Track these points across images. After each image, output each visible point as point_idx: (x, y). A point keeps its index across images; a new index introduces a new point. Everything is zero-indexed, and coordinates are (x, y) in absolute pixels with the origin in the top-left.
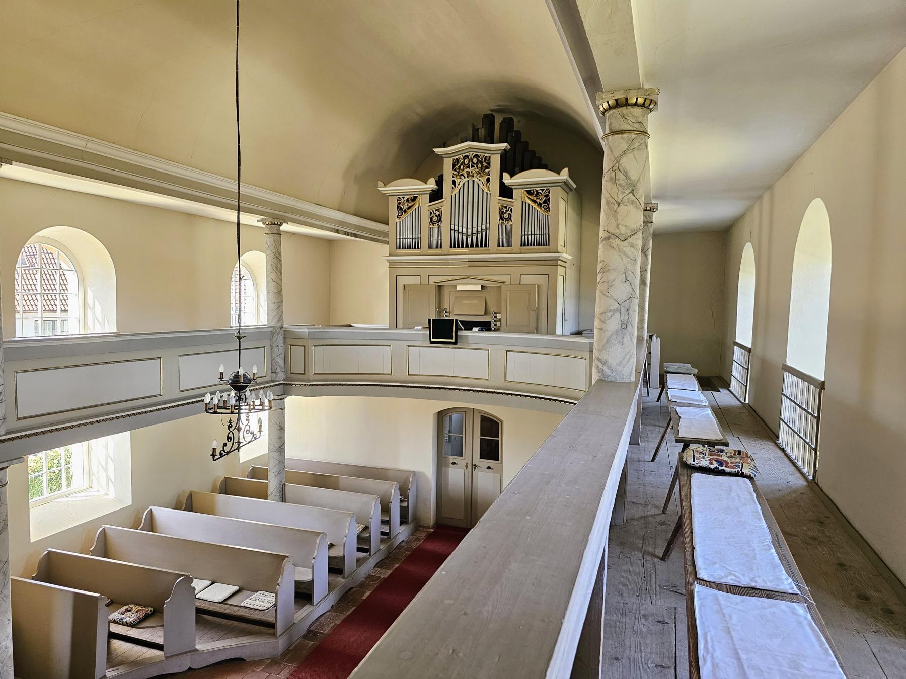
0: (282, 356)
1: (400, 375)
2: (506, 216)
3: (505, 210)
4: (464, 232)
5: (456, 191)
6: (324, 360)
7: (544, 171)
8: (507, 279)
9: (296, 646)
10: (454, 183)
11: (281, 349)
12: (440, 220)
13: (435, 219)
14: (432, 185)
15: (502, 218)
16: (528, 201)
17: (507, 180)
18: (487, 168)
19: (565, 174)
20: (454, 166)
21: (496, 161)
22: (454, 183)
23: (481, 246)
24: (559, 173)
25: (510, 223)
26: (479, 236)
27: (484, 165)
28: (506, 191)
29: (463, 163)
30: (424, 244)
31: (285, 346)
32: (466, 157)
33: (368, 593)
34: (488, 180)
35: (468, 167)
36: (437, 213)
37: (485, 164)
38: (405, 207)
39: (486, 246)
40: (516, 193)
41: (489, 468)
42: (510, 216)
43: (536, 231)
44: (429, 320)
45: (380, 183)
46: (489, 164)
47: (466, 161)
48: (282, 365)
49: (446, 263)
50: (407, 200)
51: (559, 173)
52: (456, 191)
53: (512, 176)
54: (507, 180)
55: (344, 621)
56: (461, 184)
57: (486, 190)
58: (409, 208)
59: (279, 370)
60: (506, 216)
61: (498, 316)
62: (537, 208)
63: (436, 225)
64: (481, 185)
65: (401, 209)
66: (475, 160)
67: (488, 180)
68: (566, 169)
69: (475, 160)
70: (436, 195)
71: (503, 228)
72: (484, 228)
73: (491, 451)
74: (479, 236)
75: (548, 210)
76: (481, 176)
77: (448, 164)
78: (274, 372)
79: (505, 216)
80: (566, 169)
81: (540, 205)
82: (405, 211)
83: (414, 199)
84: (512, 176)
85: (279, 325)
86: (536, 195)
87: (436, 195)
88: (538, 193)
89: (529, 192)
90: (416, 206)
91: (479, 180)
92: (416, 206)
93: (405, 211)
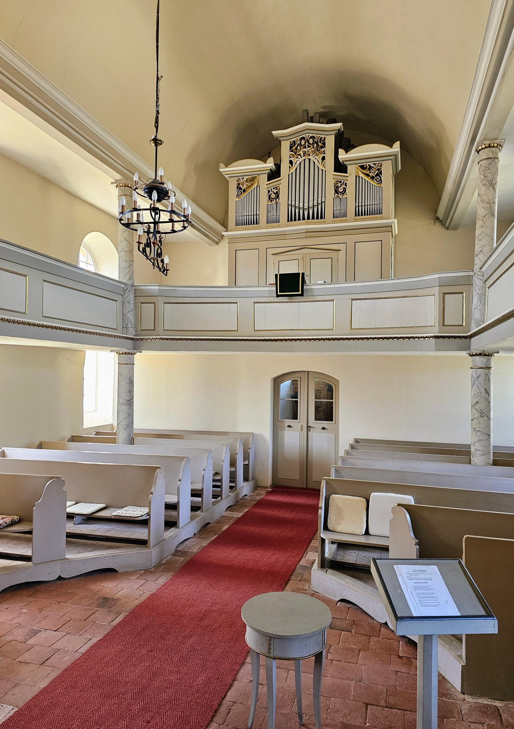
0: (133, 313)
1: (246, 332)
2: (341, 190)
3: (339, 184)
6: (174, 317)
7: (378, 145)
8: (342, 247)
9: (168, 561)
10: (291, 162)
11: (132, 306)
13: (273, 196)
14: (270, 164)
15: (336, 192)
16: (361, 175)
17: (343, 155)
18: (322, 147)
19: (396, 147)
20: (291, 148)
21: (330, 142)
22: (291, 162)
23: (317, 218)
24: (391, 147)
25: (345, 196)
26: (316, 209)
27: (320, 145)
28: (340, 167)
29: (300, 144)
30: (263, 219)
31: (135, 303)
32: (303, 138)
33: (225, 527)
34: (323, 158)
35: (305, 147)
36: (275, 191)
37: (320, 144)
39: (321, 218)
40: (349, 168)
41: (324, 428)
42: (345, 189)
43: (370, 202)
44: (276, 275)
45: (222, 165)
46: (324, 144)
47: (303, 142)
48: (133, 322)
49: (283, 235)
51: (391, 147)
52: (293, 170)
53: (347, 152)
54: (343, 155)
55: (209, 544)
56: (298, 163)
57: (321, 167)
58: (249, 187)
59: (129, 325)
60: (341, 190)
62: (370, 181)
63: (274, 202)
64: (317, 163)
65: (241, 189)
66: (311, 141)
67: (323, 158)
68: (399, 142)
69: (311, 141)
70: (274, 174)
71: (338, 201)
72: (320, 202)
73: (326, 412)
74: (316, 209)
75: (380, 181)
76: (317, 155)
77: (285, 146)
78: (125, 327)
79: (339, 190)
80: (399, 142)
81: (373, 178)
82: (244, 191)
84: (347, 152)
85: (130, 282)
86: (369, 169)
87: (274, 174)
88: (370, 167)
89: (362, 167)
90: (255, 185)
91: (315, 159)
92: (255, 185)
93: (244, 191)
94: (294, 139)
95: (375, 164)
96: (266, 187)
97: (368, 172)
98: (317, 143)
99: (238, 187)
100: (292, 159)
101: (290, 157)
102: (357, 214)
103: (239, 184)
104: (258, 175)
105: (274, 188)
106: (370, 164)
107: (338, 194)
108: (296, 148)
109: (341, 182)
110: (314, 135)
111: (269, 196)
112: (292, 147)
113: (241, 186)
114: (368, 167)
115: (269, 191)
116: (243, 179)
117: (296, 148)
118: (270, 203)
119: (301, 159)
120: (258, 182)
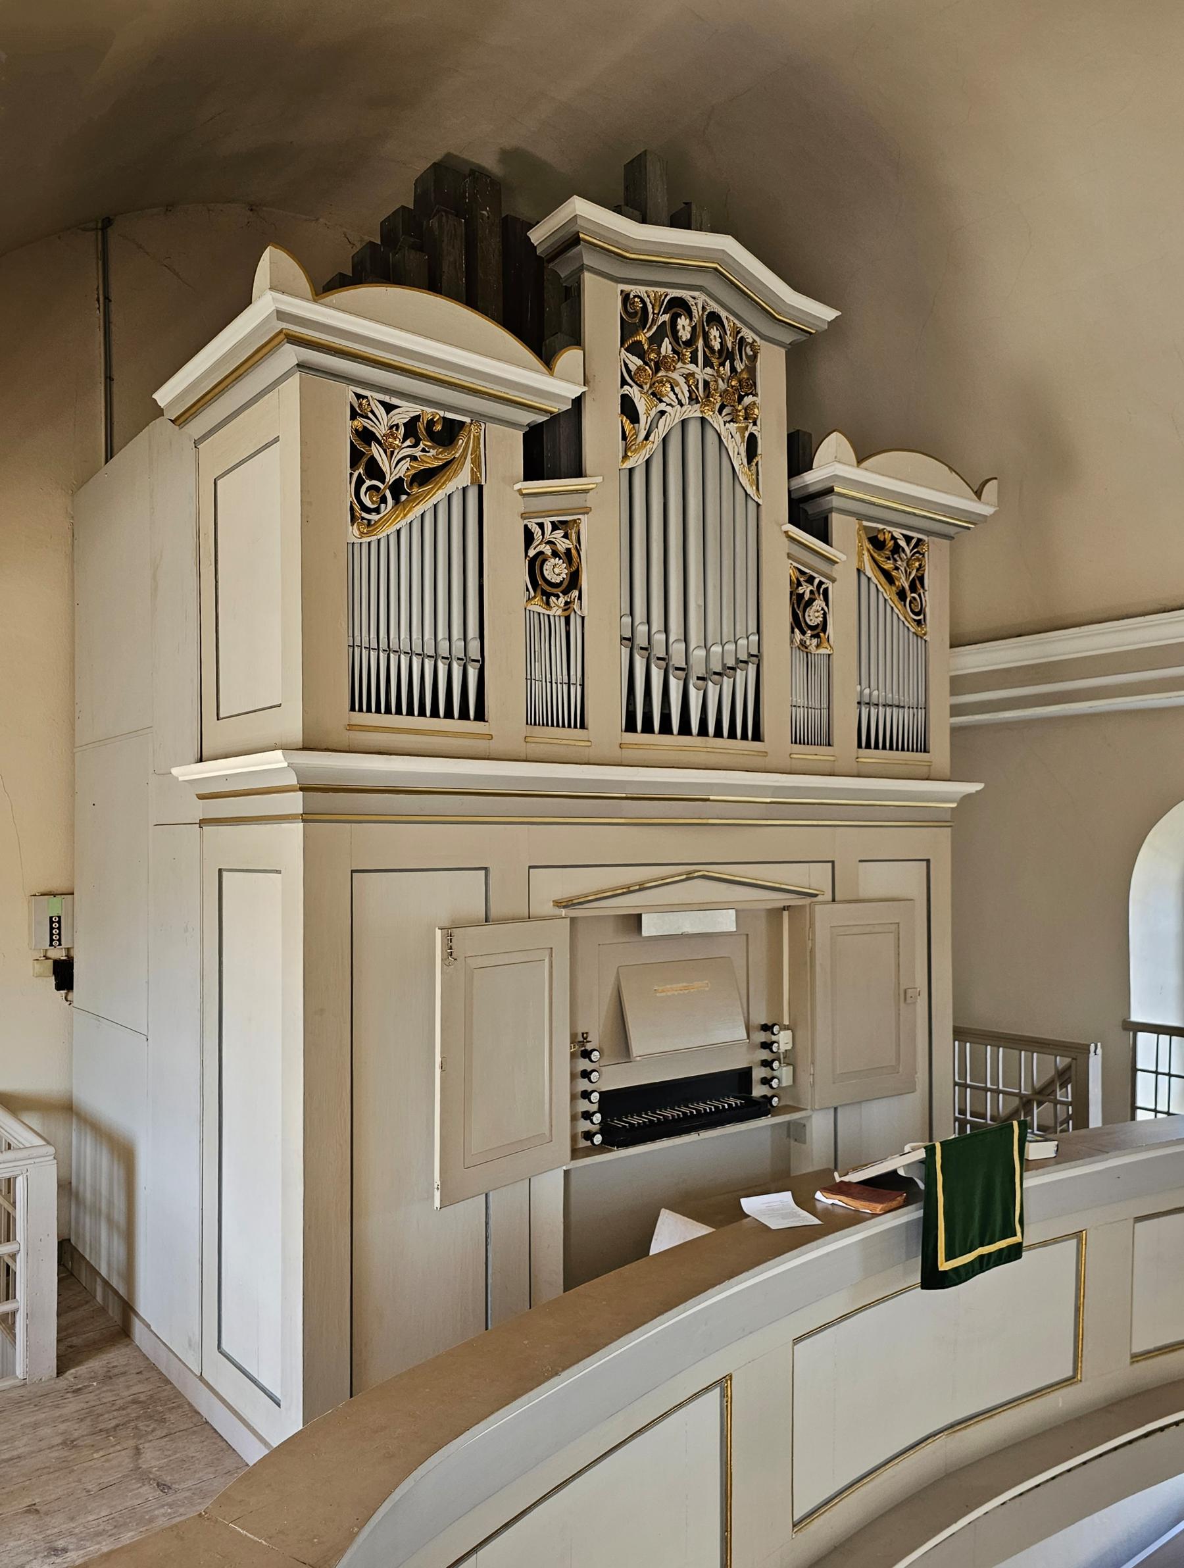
2: (813, 616)
3: (806, 589)
4: (678, 660)
5: (637, 460)
10: (629, 409)
12: (574, 581)
15: (797, 623)
20: (627, 330)
22: (629, 409)
28: (810, 513)
36: (563, 545)
38: (404, 470)
50: (411, 427)
58: (425, 477)
61: (783, 1040)
65: (374, 470)
82: (397, 488)
83: (448, 433)
88: (897, 549)
92: (463, 478)
94: (641, 290)
95: (908, 539)
96: (521, 505)
97: (888, 566)
98: (730, 356)
99: (356, 457)
100: (634, 392)
101: (624, 382)
102: (866, 742)
103: (366, 436)
104: (480, 418)
105: (555, 527)
106: (897, 533)
107: (803, 633)
108: (656, 340)
109: (810, 580)
110: (724, 314)
111: (532, 562)
112: (636, 333)
113: (376, 451)
114: (891, 544)
115: (529, 537)
116: (389, 408)
117: (656, 340)
118: (537, 607)
119: (675, 414)
120: (476, 462)
